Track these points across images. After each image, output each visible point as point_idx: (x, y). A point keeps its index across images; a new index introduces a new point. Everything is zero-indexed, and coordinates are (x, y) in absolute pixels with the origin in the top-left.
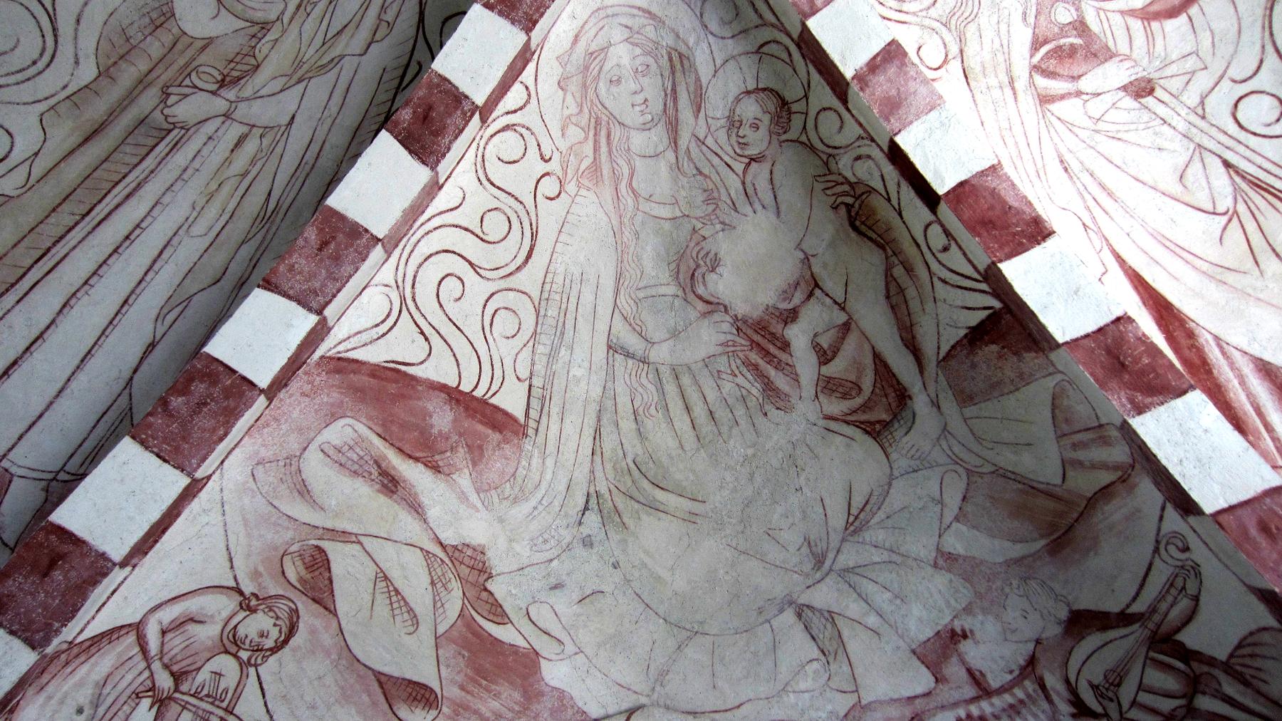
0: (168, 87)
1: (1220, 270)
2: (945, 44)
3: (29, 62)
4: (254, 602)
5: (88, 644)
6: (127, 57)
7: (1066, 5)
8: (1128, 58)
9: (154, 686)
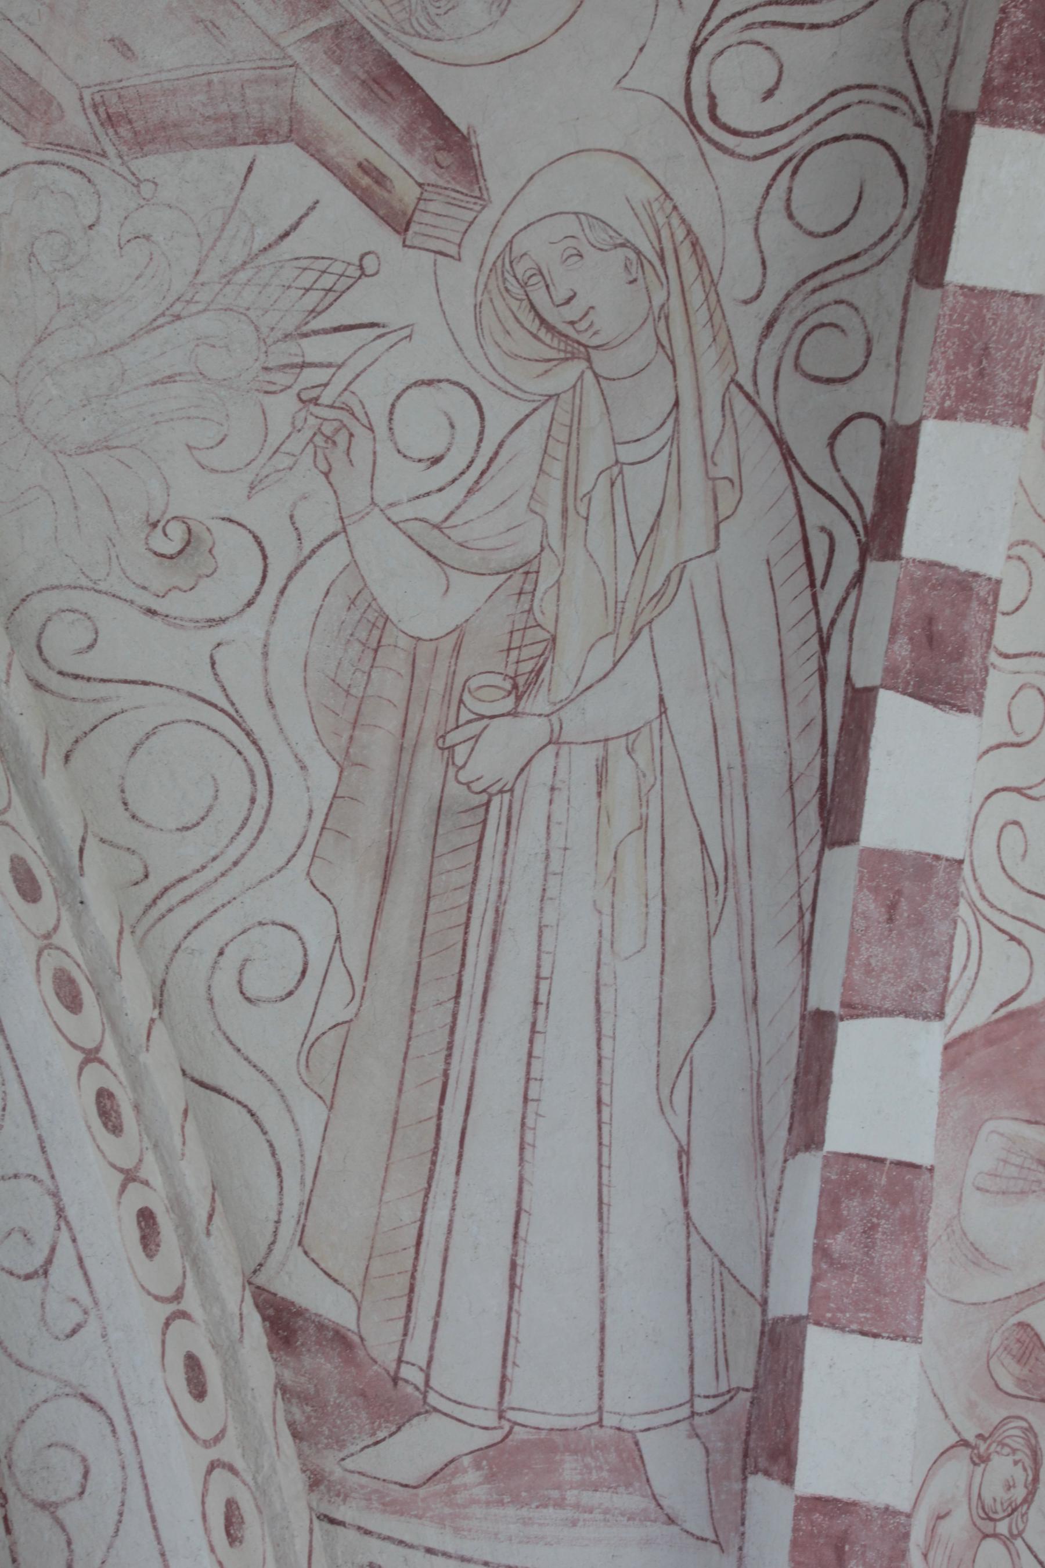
0: (443, 737)
3: (247, 804)
6: (361, 721)
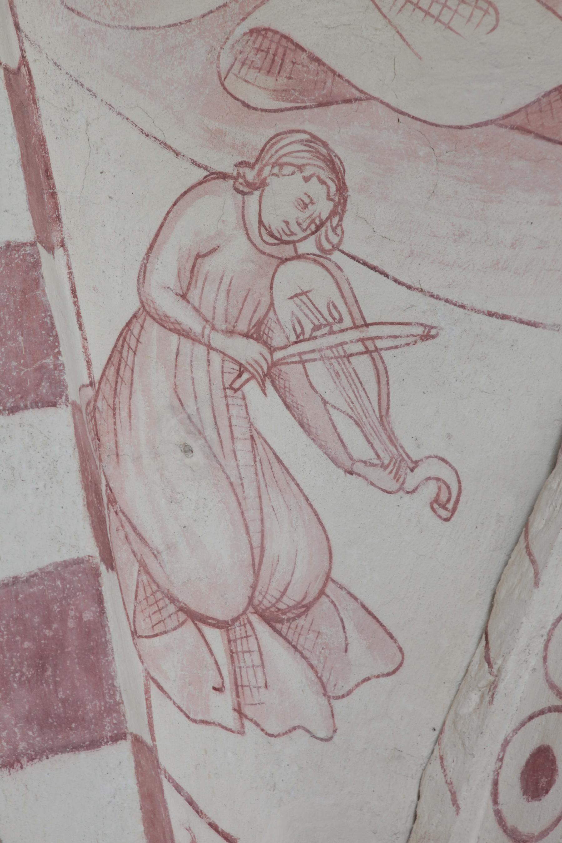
4: (250, 175)
5: (111, 371)
9: (240, 365)
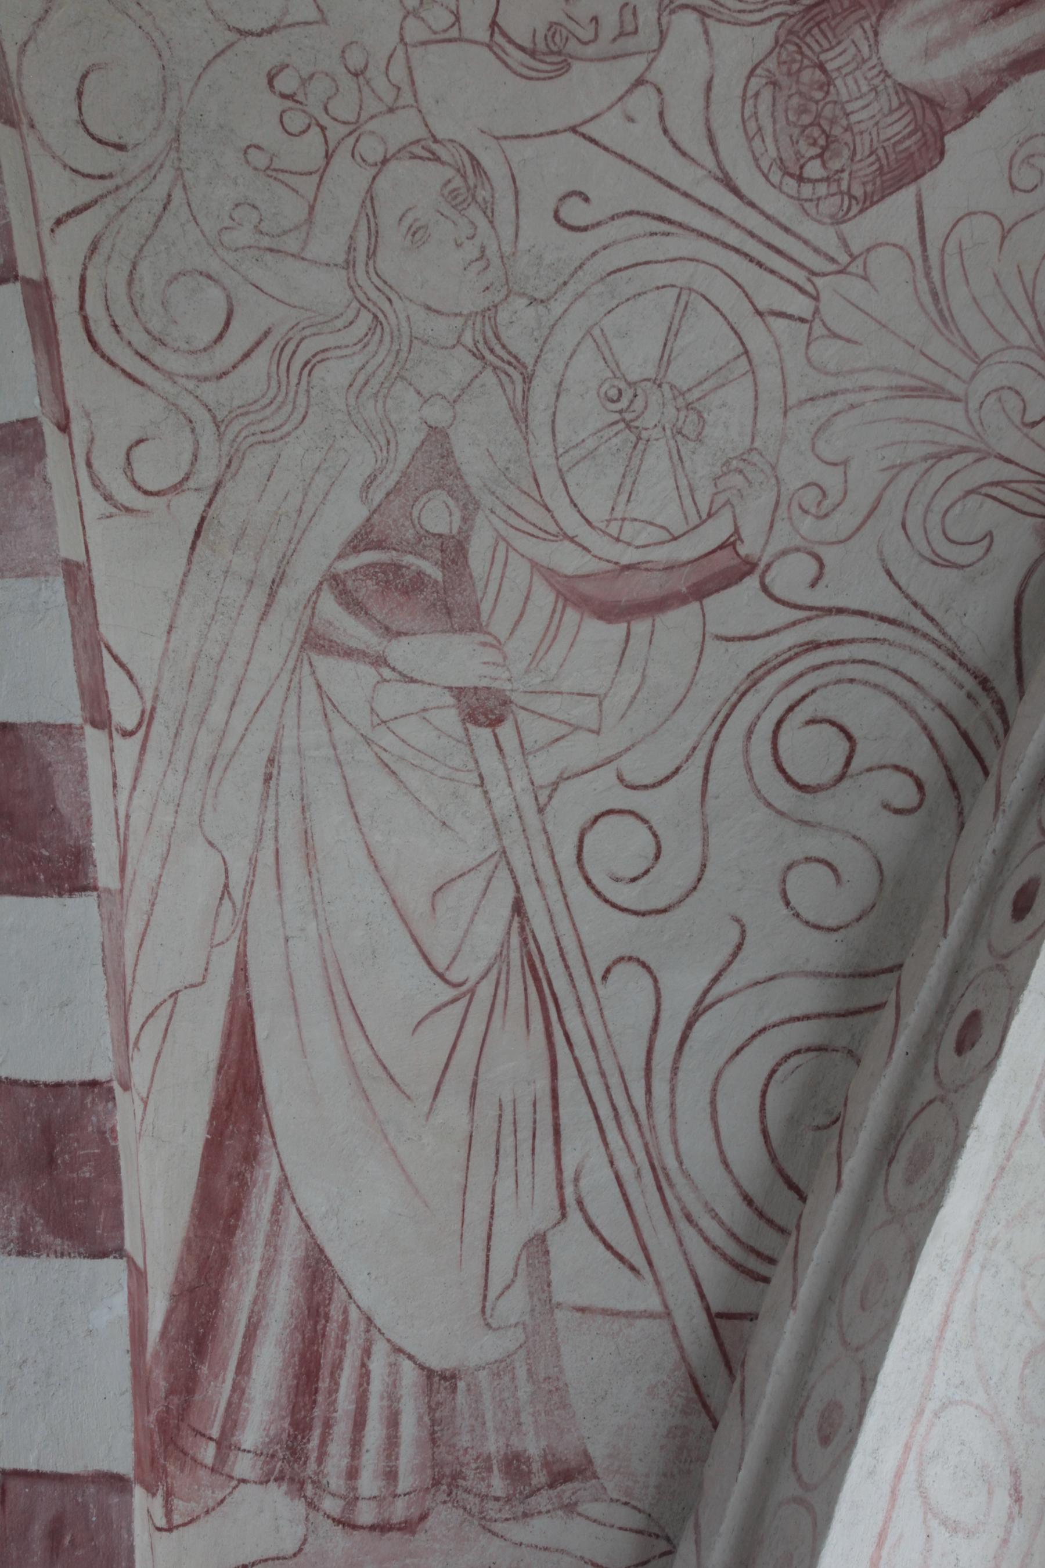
1: (379, 1071)
2: (195, 457)
7: (451, 503)
8: (498, 645)
